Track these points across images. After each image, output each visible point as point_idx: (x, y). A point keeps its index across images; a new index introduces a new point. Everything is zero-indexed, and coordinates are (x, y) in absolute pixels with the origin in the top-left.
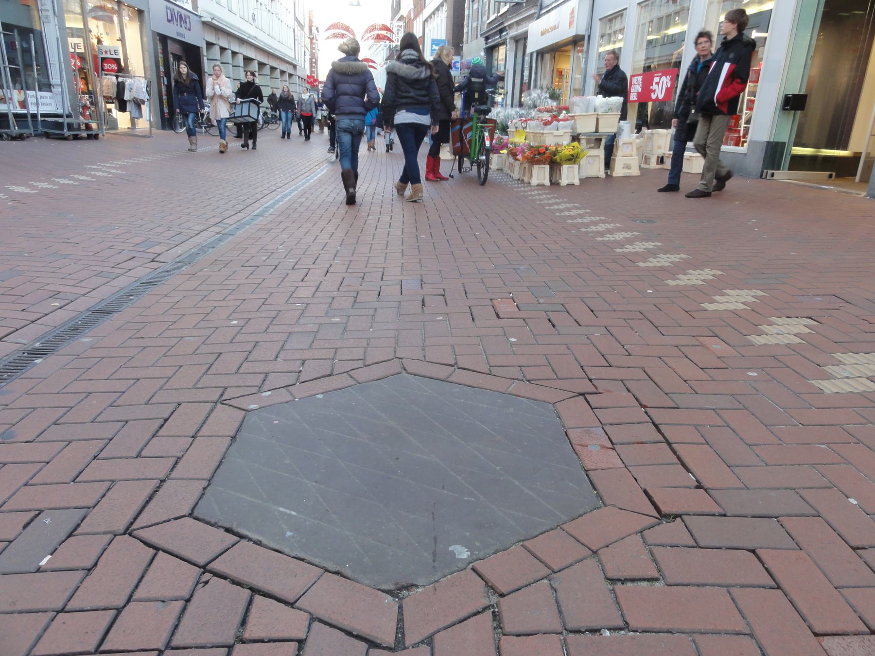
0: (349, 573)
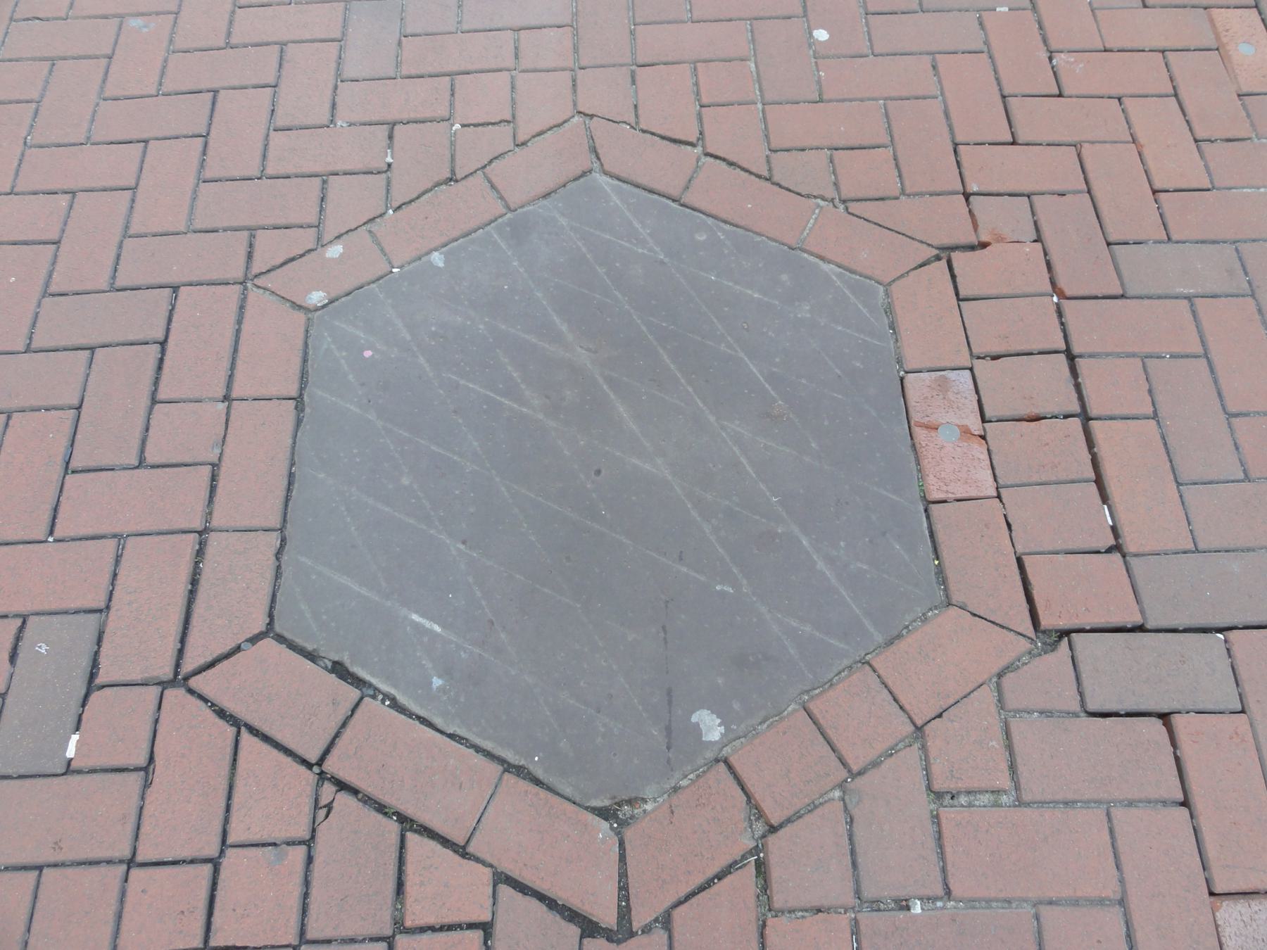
0: (539, 773)
